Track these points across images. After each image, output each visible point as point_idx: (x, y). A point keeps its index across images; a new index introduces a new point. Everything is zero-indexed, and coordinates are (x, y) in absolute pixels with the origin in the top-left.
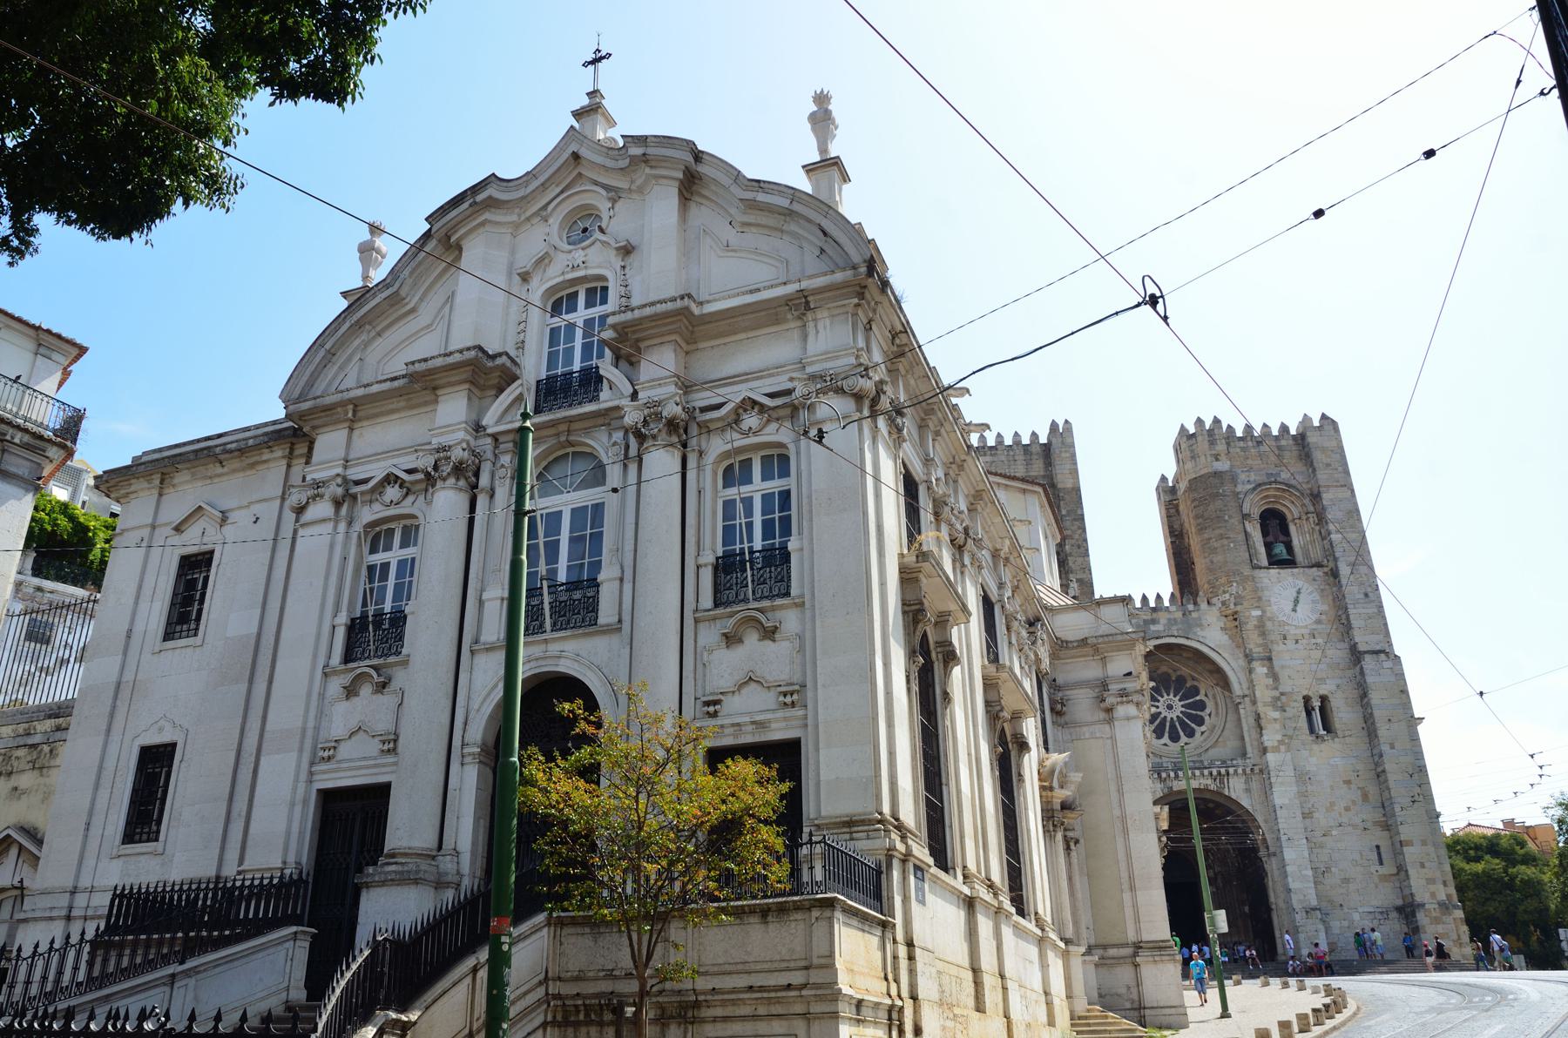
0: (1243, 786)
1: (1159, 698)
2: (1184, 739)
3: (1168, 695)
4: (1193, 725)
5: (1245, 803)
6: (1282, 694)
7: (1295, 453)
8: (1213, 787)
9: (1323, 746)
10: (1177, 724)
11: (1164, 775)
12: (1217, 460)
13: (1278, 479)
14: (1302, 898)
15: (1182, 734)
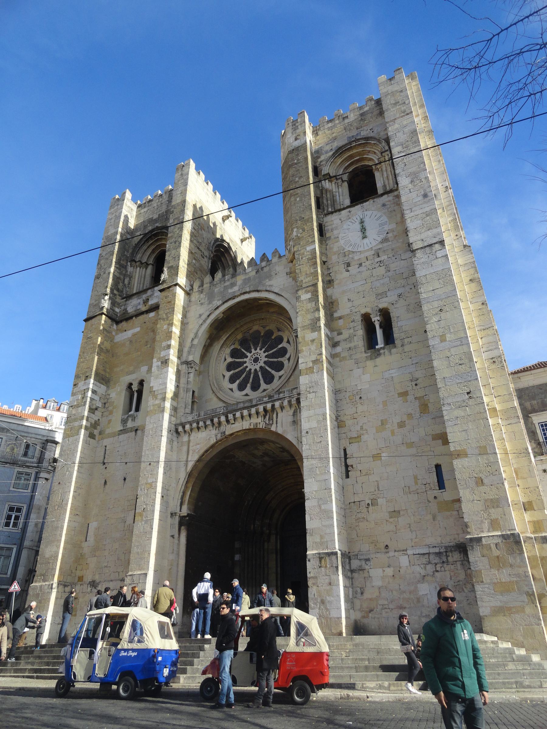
0: (290, 419)
1: (248, 354)
2: (263, 386)
3: (256, 350)
4: (273, 372)
5: (290, 436)
6: (340, 318)
7: (376, 112)
8: (262, 425)
9: (378, 360)
10: (260, 374)
11: (216, 420)
12: (296, 139)
13: (357, 138)
14: (318, 540)
15: (262, 382)
